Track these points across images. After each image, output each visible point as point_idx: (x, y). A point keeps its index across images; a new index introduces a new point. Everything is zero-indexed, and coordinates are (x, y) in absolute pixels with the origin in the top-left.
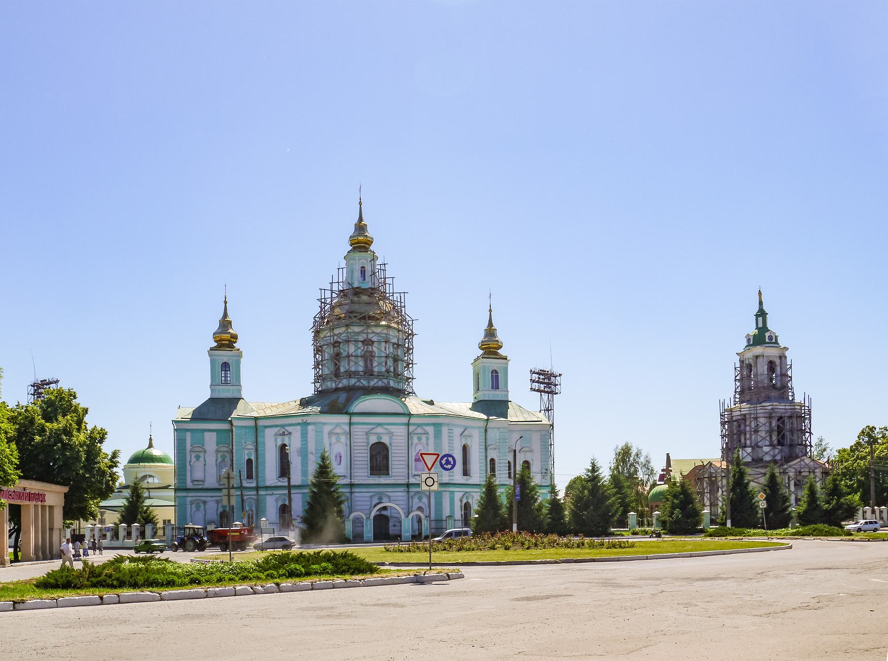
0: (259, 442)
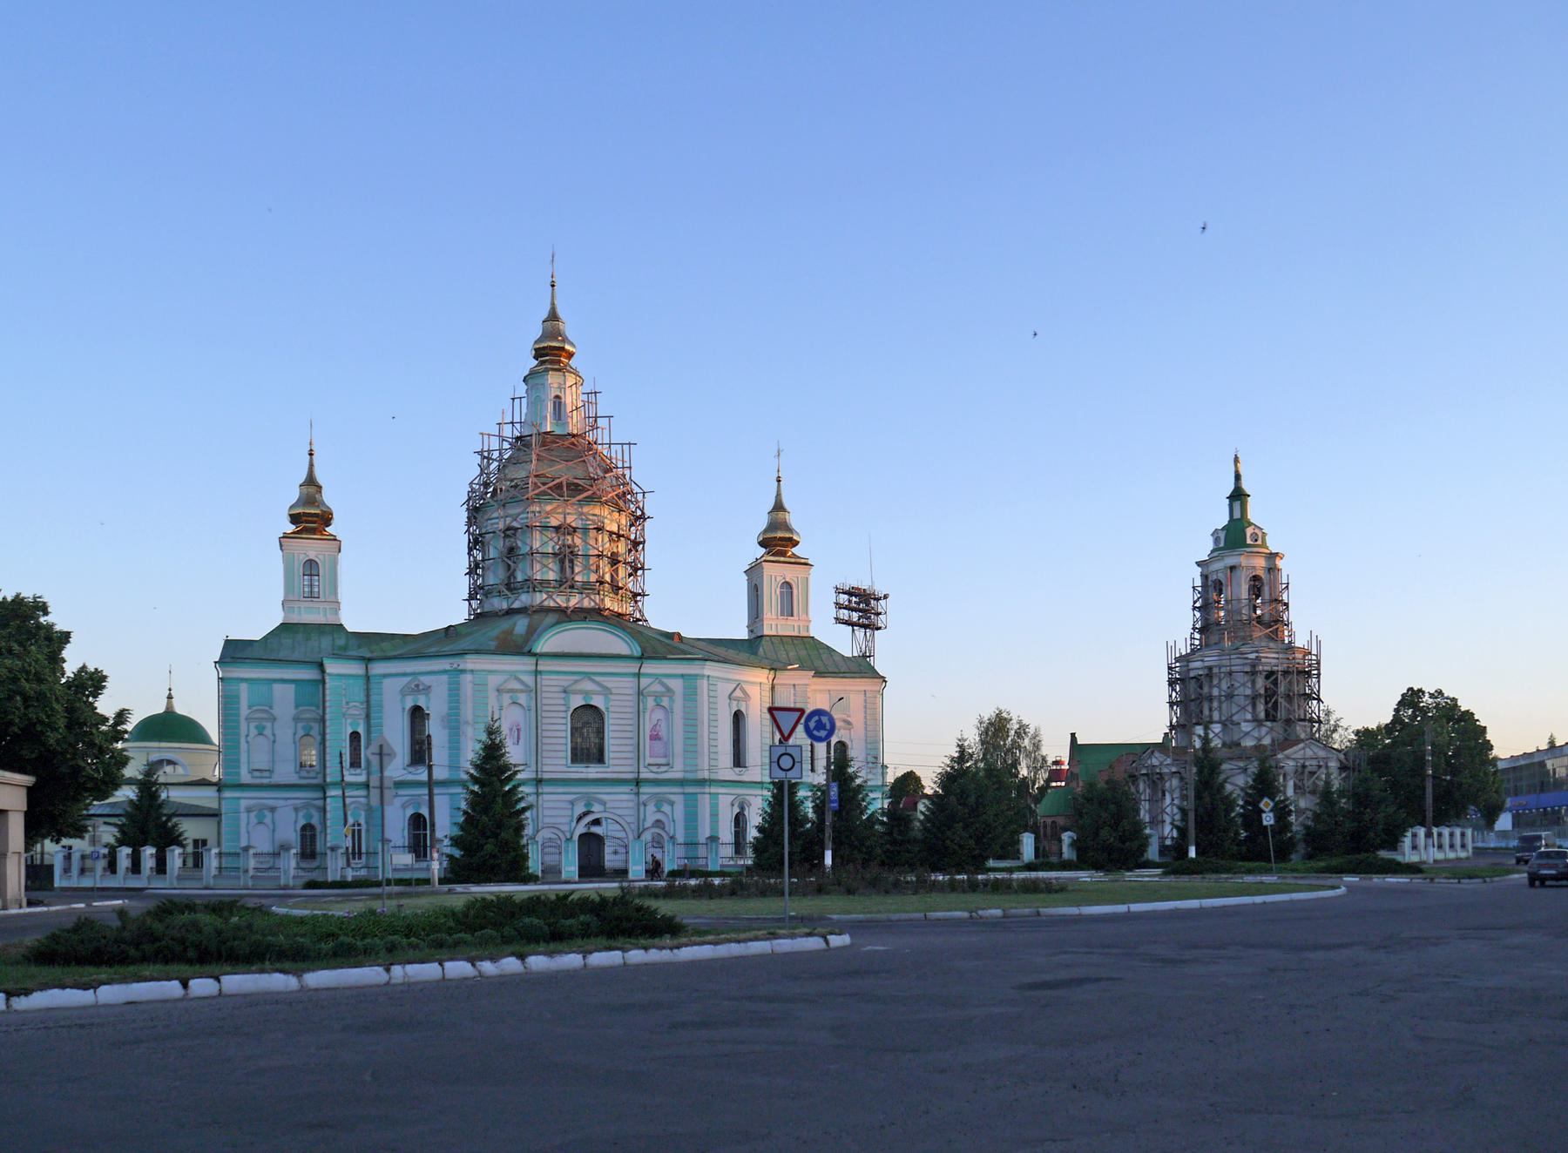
0: (372, 702)
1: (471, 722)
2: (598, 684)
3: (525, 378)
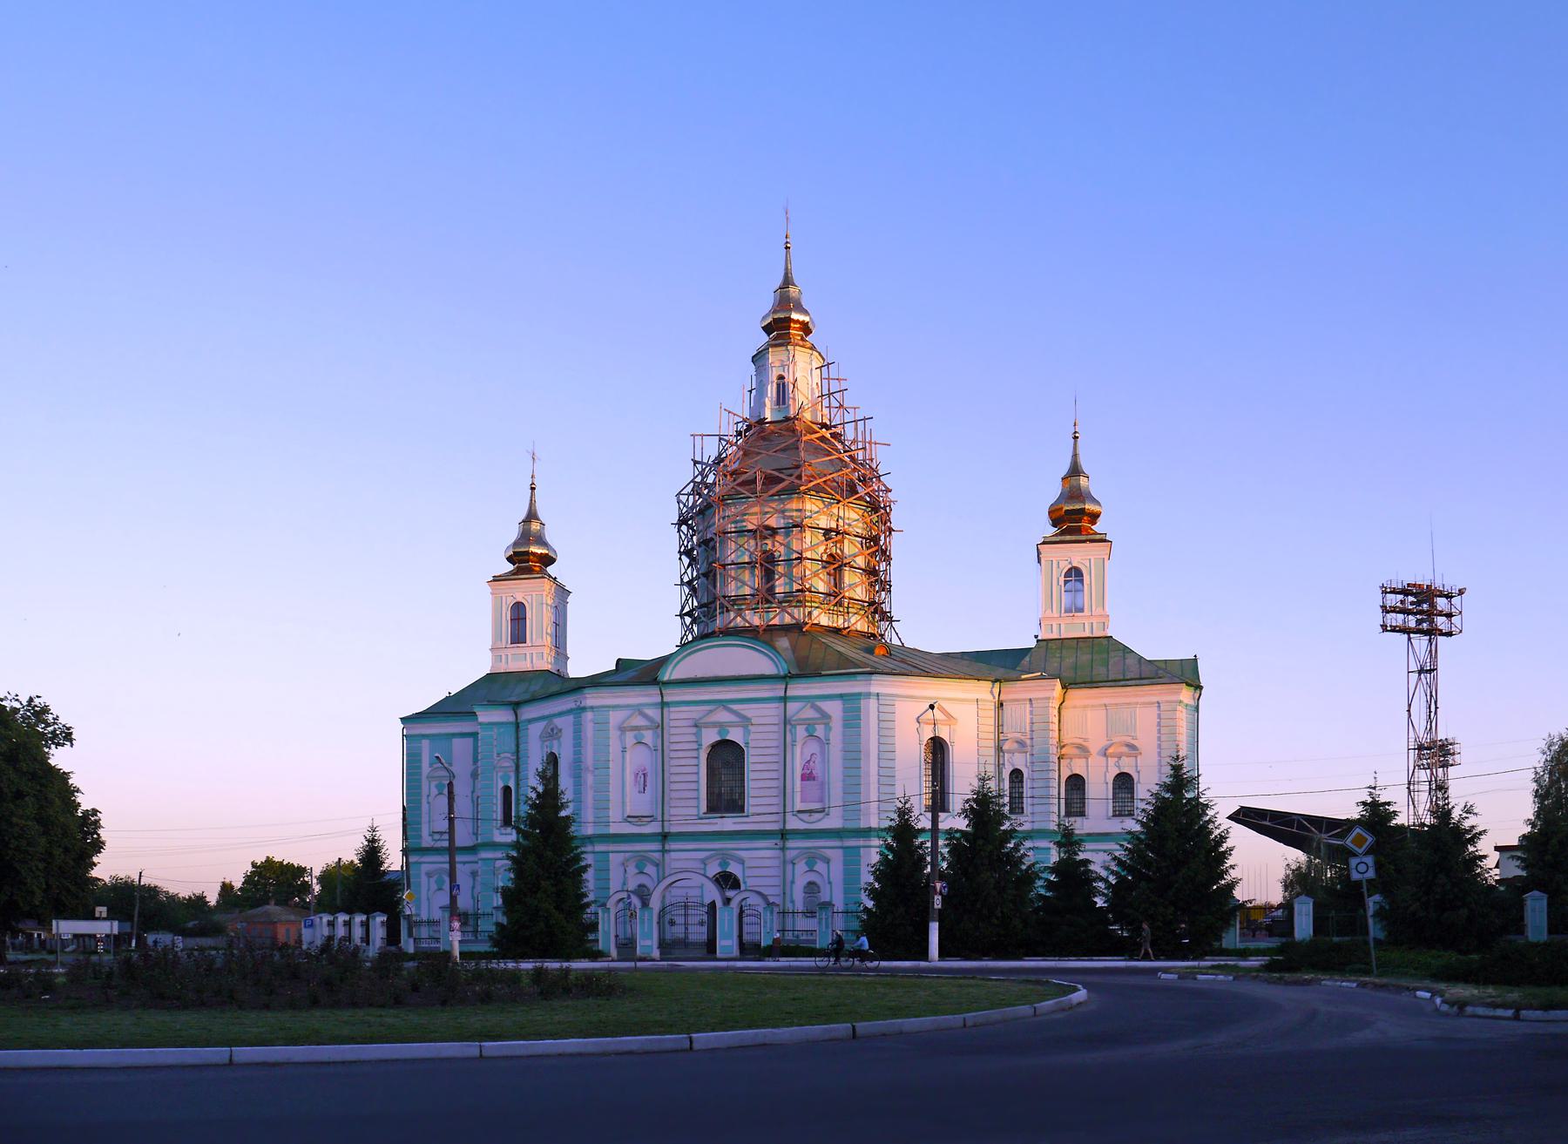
1: (591, 769)
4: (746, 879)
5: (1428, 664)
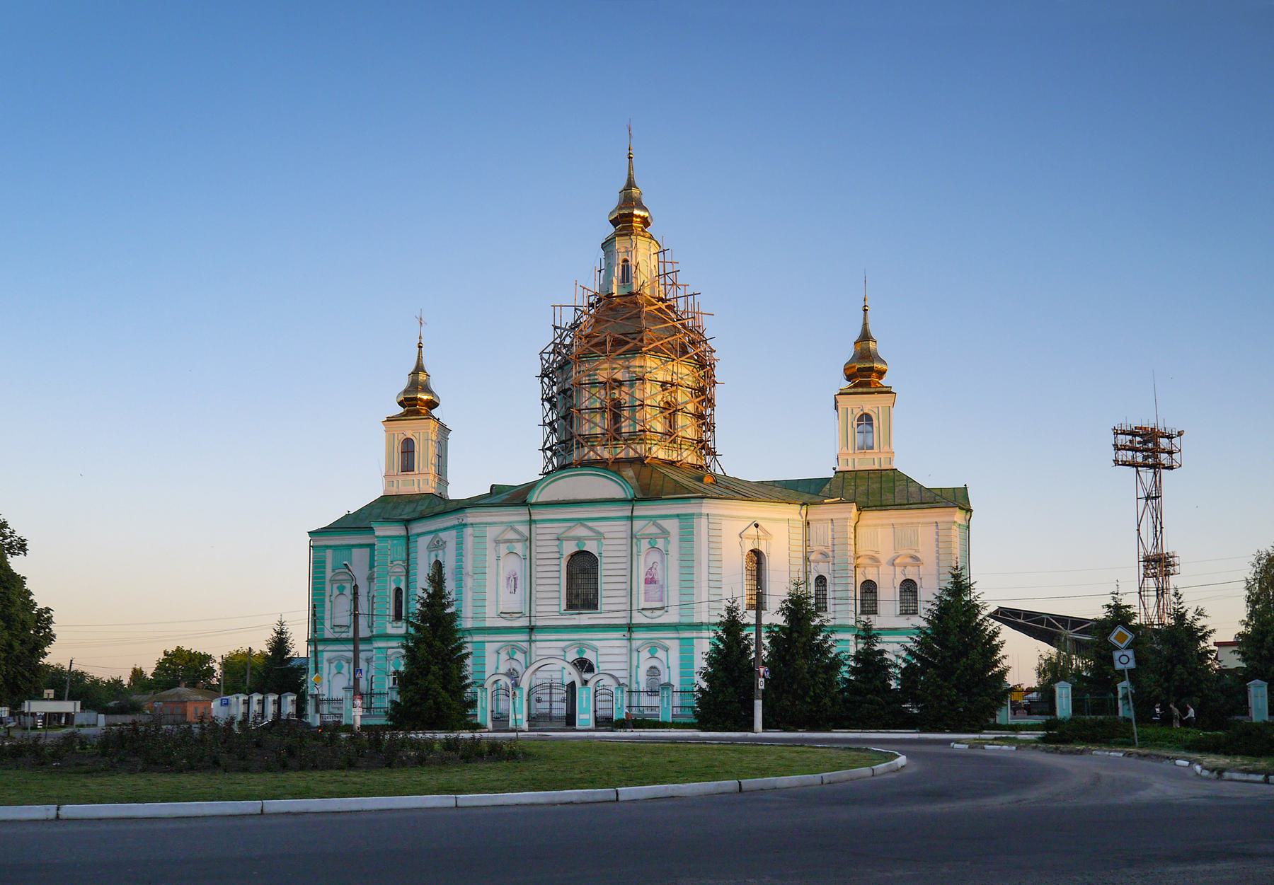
2: (590, 529)
3: (602, 244)
4: (599, 664)
5: (1154, 492)
